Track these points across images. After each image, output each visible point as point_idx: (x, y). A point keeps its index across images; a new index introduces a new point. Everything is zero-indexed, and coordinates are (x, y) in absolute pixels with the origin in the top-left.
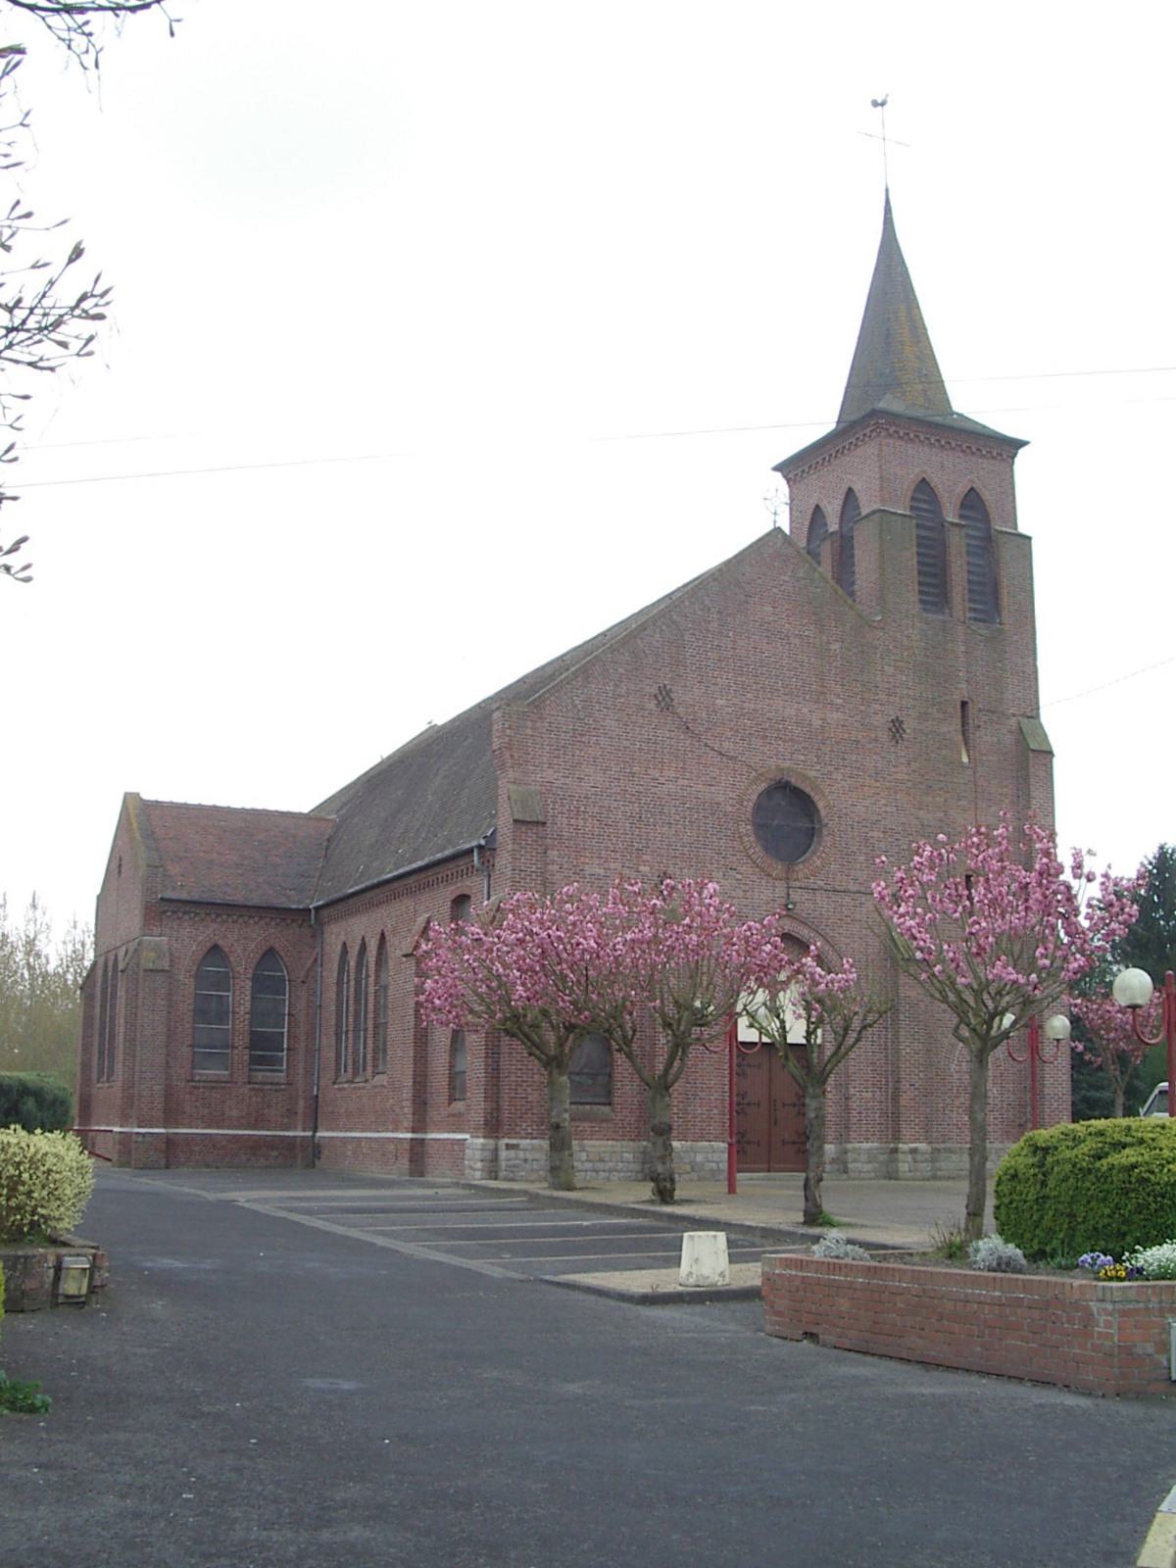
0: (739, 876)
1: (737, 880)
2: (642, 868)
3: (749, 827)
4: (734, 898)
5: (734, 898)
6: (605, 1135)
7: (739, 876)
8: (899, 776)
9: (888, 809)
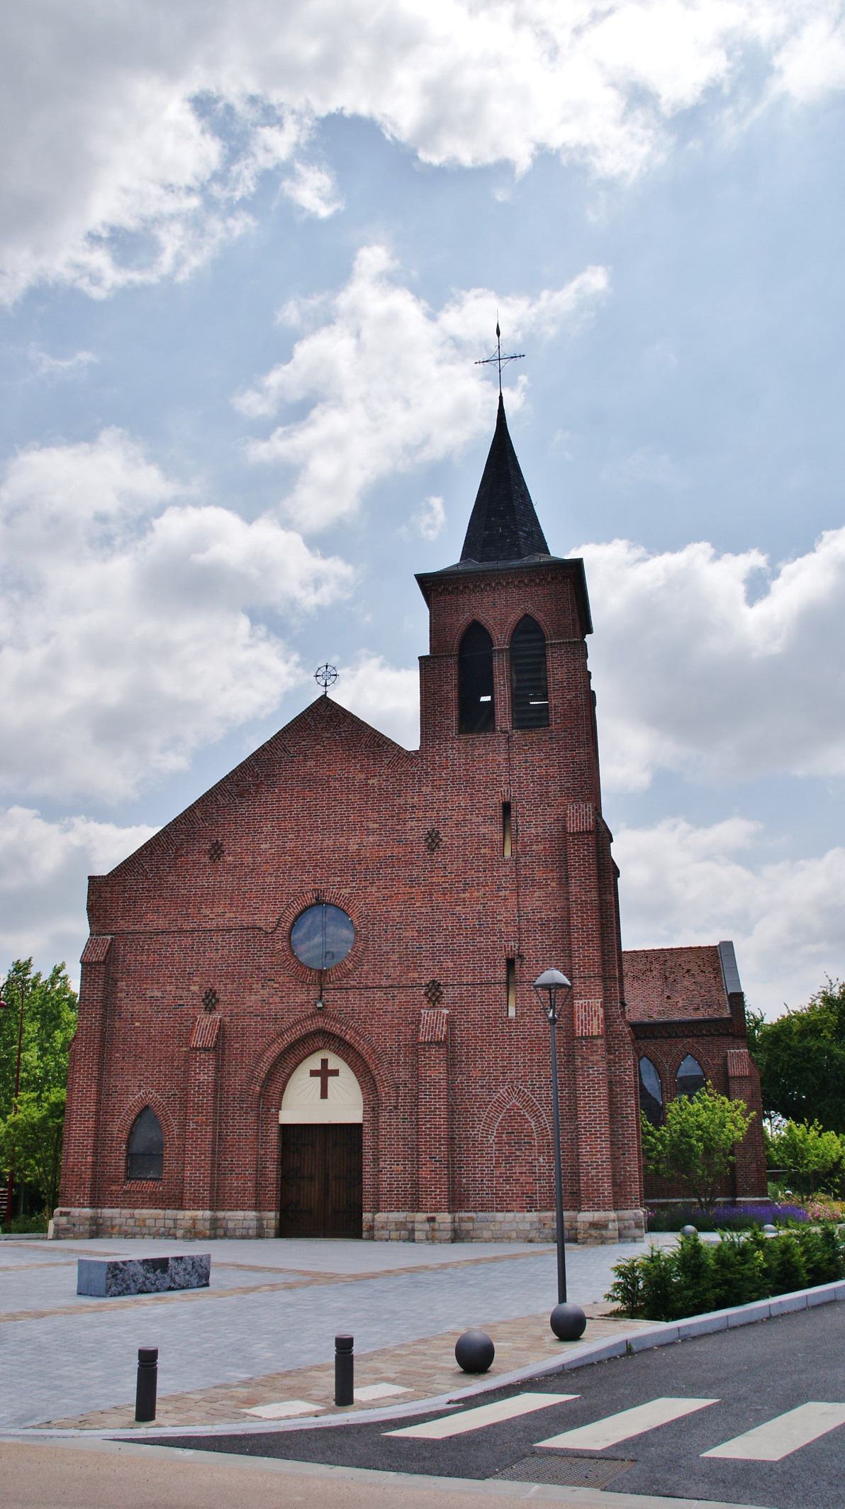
0: (277, 985)
1: (275, 988)
2: (192, 988)
3: (284, 944)
4: (271, 1004)
5: (271, 1004)
6: (154, 1205)
7: (277, 985)
8: (434, 880)
9: (423, 910)
